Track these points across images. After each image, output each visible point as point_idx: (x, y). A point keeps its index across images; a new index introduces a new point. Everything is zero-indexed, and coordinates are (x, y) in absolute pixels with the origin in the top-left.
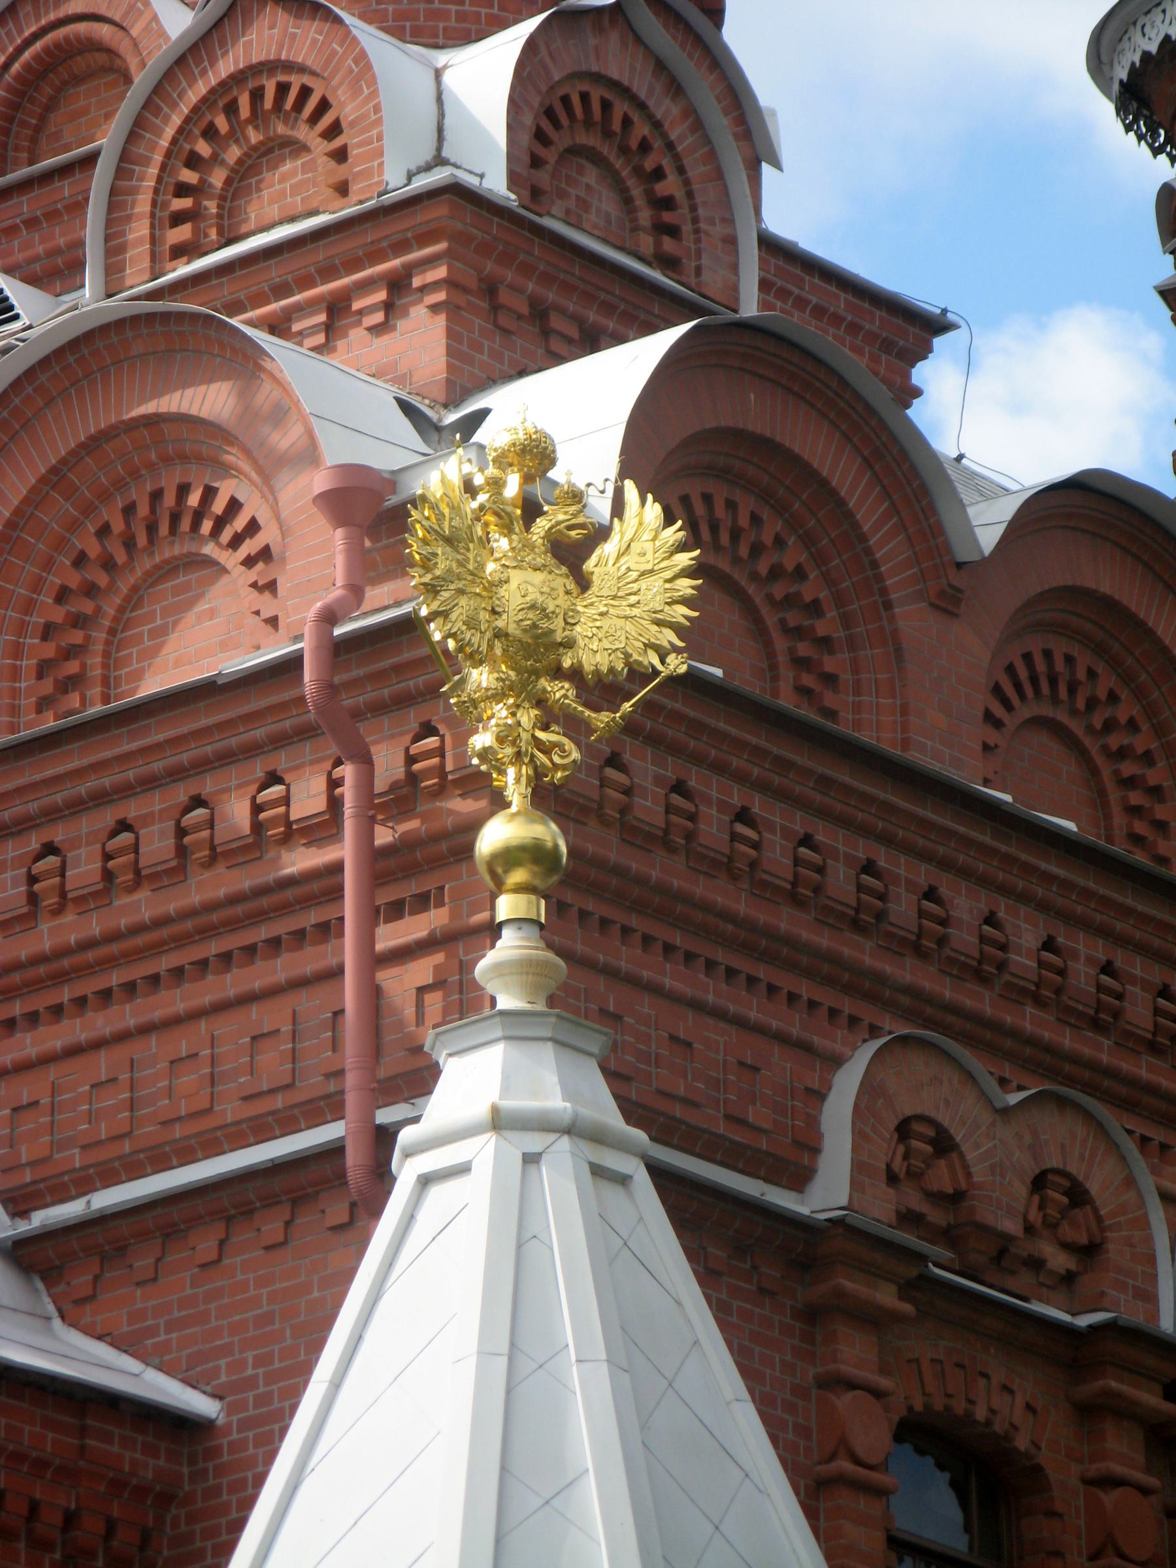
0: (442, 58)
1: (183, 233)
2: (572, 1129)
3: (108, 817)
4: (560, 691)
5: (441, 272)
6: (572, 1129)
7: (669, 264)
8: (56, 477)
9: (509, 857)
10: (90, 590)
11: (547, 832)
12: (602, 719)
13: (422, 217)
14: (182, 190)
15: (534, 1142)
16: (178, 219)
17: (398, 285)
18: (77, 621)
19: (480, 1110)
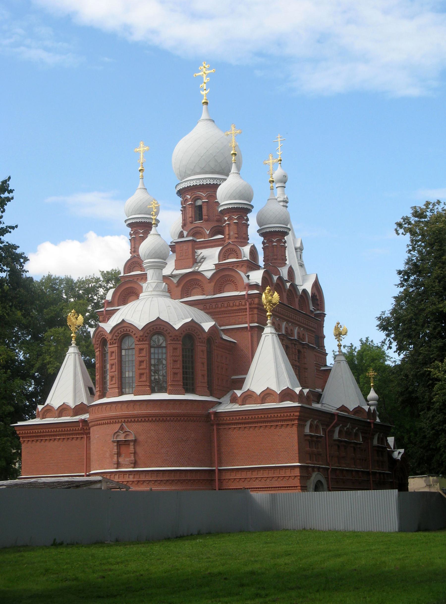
0: (243, 248)
1: (225, 258)
2: (275, 334)
3: (227, 302)
4: (271, 304)
5: (246, 265)
6: (275, 334)
7: (254, 261)
8: (221, 277)
9: (269, 315)
10: (222, 284)
11: (271, 314)
12: (274, 307)
13: (245, 261)
14: (224, 255)
15: (273, 334)
16: (224, 257)
17: (242, 265)
18: (221, 286)
19: (270, 332)
